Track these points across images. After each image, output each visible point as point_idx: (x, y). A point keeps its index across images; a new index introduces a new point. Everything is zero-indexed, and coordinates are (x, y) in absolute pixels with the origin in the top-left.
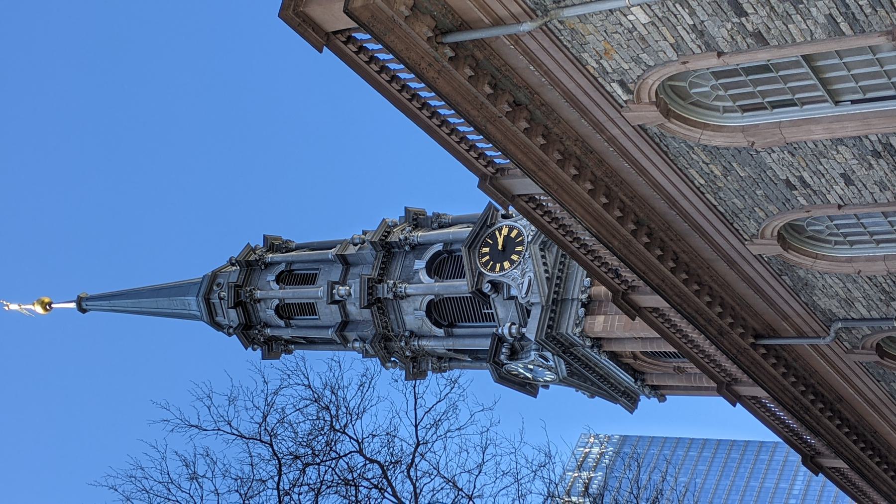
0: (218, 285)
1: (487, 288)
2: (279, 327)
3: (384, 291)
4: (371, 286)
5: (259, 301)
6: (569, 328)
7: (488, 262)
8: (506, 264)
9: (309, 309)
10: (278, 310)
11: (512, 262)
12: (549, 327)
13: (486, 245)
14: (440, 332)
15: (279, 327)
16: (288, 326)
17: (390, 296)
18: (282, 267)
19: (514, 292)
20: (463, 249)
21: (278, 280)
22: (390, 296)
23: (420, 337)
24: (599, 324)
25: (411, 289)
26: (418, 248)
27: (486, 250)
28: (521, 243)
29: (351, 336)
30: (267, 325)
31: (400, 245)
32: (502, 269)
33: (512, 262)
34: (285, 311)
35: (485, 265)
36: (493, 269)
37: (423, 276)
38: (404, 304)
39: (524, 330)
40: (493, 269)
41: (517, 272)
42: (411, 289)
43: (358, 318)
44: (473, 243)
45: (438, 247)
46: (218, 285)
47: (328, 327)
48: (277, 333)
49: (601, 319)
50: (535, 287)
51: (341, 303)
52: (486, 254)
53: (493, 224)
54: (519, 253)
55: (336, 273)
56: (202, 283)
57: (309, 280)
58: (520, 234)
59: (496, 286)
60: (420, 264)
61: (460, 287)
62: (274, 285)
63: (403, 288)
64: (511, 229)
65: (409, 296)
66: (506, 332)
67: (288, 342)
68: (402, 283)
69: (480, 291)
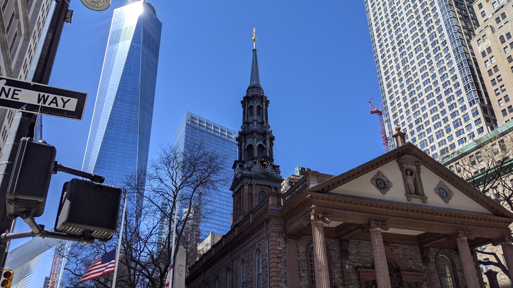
0: (258, 89)
1: (255, 161)
2: (248, 106)
3: (255, 134)
4: (256, 132)
5: (254, 101)
6: (245, 181)
7: (261, 160)
8: (260, 165)
9: (252, 114)
10: (251, 106)
11: (260, 166)
12: (246, 176)
13: (264, 160)
14: (246, 148)
15: (248, 106)
16: (248, 108)
17: (254, 136)
18: (261, 107)
19: (254, 166)
20: (264, 154)
21: (258, 106)
22: (254, 136)
23: (245, 143)
24: (246, 187)
25: (255, 141)
26: (265, 142)
27: (263, 160)
28: (265, 168)
29: (245, 125)
30: (248, 103)
31: (266, 137)
32: (259, 164)
33: (260, 166)
34: (251, 107)
35: (260, 160)
36: (259, 162)
37: (258, 144)
38: (252, 139)
39: (245, 170)
40: (259, 162)
41: (258, 168)
42: (255, 141)
43: (249, 126)
44: (265, 157)
45: (265, 147)
46: (258, 89)
47: (247, 119)
48: (246, 105)
49: (247, 187)
50: (254, 172)
51: (252, 123)
52: (262, 159)
53: (269, 161)
54: (262, 168)
55: (260, 121)
56: (259, 85)
57: (258, 114)
58: (267, 167)
59: (255, 163)
60: (261, 142)
61: (256, 154)
62: (257, 105)
63: (256, 139)
64: (268, 165)
65: (254, 140)
66: (245, 166)
67: (245, 108)
68: (257, 139)
69: (254, 159)
